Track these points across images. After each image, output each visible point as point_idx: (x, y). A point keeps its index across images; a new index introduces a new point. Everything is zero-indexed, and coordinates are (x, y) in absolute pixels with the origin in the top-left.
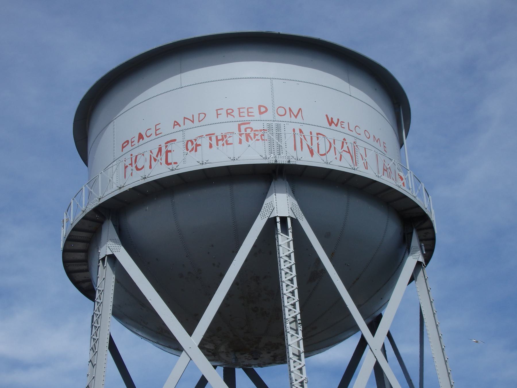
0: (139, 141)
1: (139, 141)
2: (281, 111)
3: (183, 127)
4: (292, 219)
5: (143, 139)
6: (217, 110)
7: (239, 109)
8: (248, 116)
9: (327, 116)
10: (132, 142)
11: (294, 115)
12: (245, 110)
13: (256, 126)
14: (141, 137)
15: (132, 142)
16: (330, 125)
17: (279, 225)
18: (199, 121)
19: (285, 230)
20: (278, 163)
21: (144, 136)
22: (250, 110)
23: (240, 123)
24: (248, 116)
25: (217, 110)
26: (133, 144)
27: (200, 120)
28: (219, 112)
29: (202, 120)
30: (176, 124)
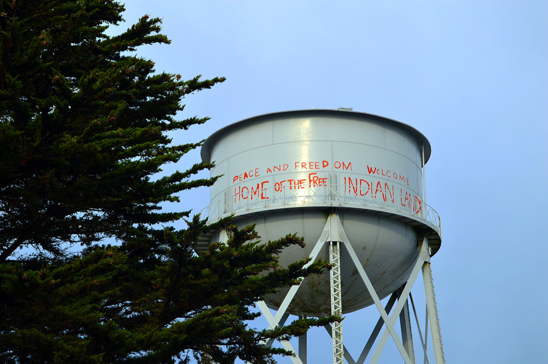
0: (244, 178)
1: (244, 178)
2: (337, 165)
4: (340, 243)
5: (247, 177)
6: (296, 163)
7: (310, 163)
8: (316, 168)
9: (368, 166)
10: (240, 178)
11: (346, 168)
12: (314, 164)
13: (321, 175)
14: (246, 175)
15: (240, 178)
16: (370, 173)
17: (331, 247)
18: (284, 170)
20: (333, 206)
21: (248, 175)
22: (317, 164)
23: (310, 173)
24: (316, 168)
25: (296, 163)
26: (241, 179)
27: (284, 169)
29: (286, 169)
30: (269, 170)
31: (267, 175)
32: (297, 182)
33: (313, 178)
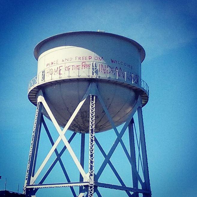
3: (65, 62)
14: (52, 63)
16: (112, 62)
19: (93, 100)
22: (86, 58)
28: (76, 58)
31: (62, 63)
32: (76, 67)
33: (84, 64)
